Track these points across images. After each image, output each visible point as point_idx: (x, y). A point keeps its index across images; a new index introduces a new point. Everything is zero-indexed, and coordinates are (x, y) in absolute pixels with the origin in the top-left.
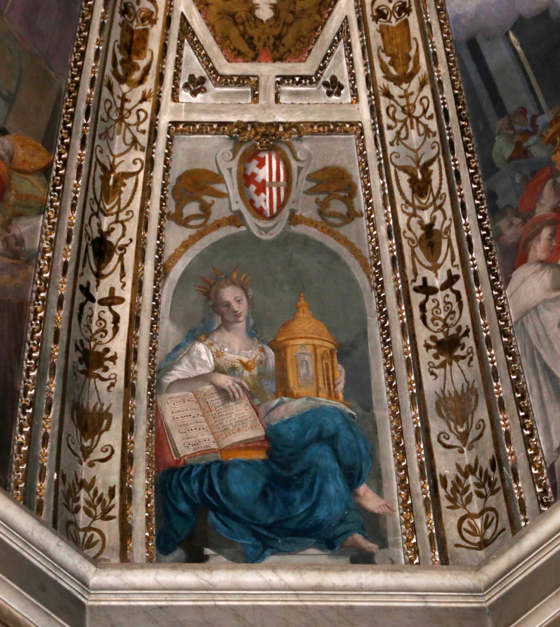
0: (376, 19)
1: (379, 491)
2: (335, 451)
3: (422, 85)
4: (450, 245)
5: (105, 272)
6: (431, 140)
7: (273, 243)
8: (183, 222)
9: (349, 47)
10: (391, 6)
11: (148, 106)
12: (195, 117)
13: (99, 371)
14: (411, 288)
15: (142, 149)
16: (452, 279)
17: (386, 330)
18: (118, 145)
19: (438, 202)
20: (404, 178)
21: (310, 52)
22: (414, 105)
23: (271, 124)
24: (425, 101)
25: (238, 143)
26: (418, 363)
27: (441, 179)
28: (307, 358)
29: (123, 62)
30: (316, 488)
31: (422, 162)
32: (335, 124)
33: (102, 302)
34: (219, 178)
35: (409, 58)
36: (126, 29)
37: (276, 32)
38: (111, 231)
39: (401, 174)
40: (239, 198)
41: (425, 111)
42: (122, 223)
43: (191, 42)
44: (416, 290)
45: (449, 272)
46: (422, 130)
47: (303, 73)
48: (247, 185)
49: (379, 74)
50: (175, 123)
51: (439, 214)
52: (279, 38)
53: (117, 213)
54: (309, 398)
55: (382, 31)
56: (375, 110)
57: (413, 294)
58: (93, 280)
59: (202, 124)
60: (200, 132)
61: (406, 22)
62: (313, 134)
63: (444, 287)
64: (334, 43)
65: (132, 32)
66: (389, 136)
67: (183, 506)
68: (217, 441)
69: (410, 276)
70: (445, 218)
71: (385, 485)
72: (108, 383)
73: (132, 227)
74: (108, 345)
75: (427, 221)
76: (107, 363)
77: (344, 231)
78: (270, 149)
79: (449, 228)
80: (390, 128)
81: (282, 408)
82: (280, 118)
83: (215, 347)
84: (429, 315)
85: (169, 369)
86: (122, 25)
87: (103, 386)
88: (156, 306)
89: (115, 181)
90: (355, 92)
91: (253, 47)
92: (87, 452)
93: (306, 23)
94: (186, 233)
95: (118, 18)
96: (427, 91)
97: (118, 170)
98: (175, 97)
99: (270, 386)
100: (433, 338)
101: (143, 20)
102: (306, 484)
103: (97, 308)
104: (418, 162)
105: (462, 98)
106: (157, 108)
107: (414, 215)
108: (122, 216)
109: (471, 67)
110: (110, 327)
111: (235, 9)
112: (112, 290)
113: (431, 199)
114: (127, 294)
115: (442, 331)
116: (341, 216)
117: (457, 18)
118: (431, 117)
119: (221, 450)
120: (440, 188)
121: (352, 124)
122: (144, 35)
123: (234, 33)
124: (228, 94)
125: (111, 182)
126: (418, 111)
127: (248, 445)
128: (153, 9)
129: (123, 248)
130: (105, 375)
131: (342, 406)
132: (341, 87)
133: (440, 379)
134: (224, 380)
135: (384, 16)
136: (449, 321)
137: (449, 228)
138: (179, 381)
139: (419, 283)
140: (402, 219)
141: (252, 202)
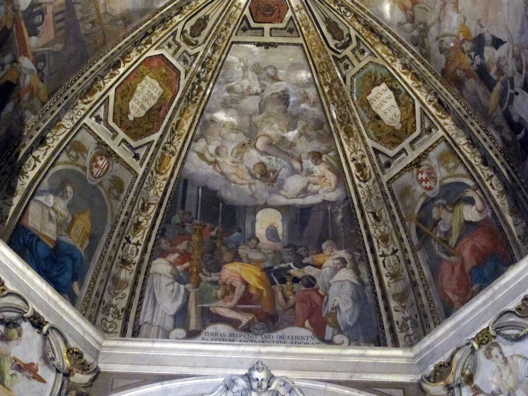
0: (163, 149)
1: (80, 288)
2: (73, 264)
3: (164, 180)
4: (144, 233)
5: (40, 149)
6: (156, 198)
7: (91, 186)
8: (69, 156)
9: (148, 150)
10: (169, 149)
11: (83, 113)
12: (92, 128)
13: (21, 177)
14: (125, 235)
15: (73, 123)
16: (138, 244)
17: (108, 242)
18: (66, 116)
19: (147, 218)
20: (141, 202)
21: (136, 140)
22: (157, 183)
23: (113, 151)
24: (162, 185)
25: (98, 147)
26: (114, 261)
27: (153, 212)
28: (80, 229)
29: (84, 93)
30: (61, 272)
31: (149, 202)
32: (131, 168)
33: (33, 157)
34: (87, 152)
35: (165, 169)
36: (92, 84)
37: (131, 126)
38: (48, 138)
39: (141, 199)
40: (88, 163)
41: (160, 188)
42: (54, 139)
43: (105, 106)
44: (126, 238)
45: (138, 241)
46: (155, 192)
47: (131, 144)
48: (93, 162)
49: (153, 165)
50: (85, 124)
51: (145, 221)
52: (130, 128)
53: (54, 135)
54: (74, 242)
55: (163, 155)
56: (145, 174)
57: (124, 238)
58: (35, 148)
59: (94, 132)
60: (90, 134)
61: (171, 158)
62: (122, 164)
63: (133, 244)
64: (145, 145)
65: (92, 87)
66: (145, 185)
67: (21, 241)
68: (41, 229)
69: (126, 232)
70: (147, 224)
71: (83, 287)
72: (21, 183)
73: (56, 144)
74: (28, 172)
75: (140, 220)
76: (24, 176)
77: (114, 202)
78: (107, 157)
79: (146, 228)
80: (146, 183)
81: (65, 237)
82: (116, 151)
83: (56, 201)
84: (124, 249)
85: (39, 195)
86: (92, 83)
87: (19, 182)
88: (47, 173)
89: (59, 125)
90: (141, 164)
91: (121, 124)
92: (5, 198)
93: (140, 131)
94: (68, 160)
95: (93, 79)
96: (165, 183)
97: (62, 123)
98: (90, 117)
99: (65, 227)
100: (122, 256)
101: (98, 87)
102: (60, 267)
103: (31, 158)
104: (148, 200)
105: (173, 194)
106: (84, 116)
107: (137, 215)
108: (55, 137)
109: (181, 186)
110: (32, 166)
111: (123, 108)
112: (39, 156)
113: (145, 215)
114: (43, 161)
115: (126, 256)
116: (115, 196)
117: (186, 170)
118: (161, 191)
119: (41, 234)
120: (150, 214)
121: (135, 172)
122: (95, 92)
123: (118, 115)
124: (105, 130)
125: (58, 124)
126: (157, 186)
127: (49, 239)
128: (103, 86)
129: (49, 147)
130: (22, 180)
131: (83, 253)
132: (139, 159)
133: (118, 270)
134: (53, 213)
135: (165, 150)
136: (130, 255)
137: (146, 228)
138: (39, 201)
139: (127, 236)
140: (134, 213)
141: (92, 168)
